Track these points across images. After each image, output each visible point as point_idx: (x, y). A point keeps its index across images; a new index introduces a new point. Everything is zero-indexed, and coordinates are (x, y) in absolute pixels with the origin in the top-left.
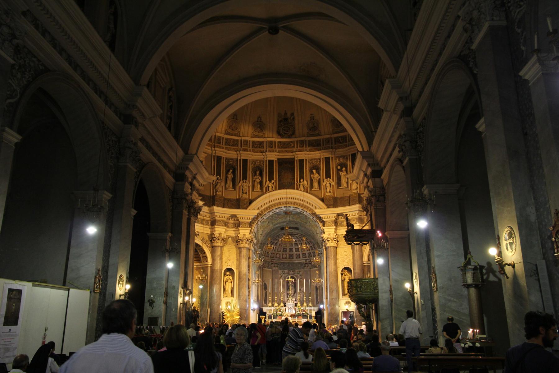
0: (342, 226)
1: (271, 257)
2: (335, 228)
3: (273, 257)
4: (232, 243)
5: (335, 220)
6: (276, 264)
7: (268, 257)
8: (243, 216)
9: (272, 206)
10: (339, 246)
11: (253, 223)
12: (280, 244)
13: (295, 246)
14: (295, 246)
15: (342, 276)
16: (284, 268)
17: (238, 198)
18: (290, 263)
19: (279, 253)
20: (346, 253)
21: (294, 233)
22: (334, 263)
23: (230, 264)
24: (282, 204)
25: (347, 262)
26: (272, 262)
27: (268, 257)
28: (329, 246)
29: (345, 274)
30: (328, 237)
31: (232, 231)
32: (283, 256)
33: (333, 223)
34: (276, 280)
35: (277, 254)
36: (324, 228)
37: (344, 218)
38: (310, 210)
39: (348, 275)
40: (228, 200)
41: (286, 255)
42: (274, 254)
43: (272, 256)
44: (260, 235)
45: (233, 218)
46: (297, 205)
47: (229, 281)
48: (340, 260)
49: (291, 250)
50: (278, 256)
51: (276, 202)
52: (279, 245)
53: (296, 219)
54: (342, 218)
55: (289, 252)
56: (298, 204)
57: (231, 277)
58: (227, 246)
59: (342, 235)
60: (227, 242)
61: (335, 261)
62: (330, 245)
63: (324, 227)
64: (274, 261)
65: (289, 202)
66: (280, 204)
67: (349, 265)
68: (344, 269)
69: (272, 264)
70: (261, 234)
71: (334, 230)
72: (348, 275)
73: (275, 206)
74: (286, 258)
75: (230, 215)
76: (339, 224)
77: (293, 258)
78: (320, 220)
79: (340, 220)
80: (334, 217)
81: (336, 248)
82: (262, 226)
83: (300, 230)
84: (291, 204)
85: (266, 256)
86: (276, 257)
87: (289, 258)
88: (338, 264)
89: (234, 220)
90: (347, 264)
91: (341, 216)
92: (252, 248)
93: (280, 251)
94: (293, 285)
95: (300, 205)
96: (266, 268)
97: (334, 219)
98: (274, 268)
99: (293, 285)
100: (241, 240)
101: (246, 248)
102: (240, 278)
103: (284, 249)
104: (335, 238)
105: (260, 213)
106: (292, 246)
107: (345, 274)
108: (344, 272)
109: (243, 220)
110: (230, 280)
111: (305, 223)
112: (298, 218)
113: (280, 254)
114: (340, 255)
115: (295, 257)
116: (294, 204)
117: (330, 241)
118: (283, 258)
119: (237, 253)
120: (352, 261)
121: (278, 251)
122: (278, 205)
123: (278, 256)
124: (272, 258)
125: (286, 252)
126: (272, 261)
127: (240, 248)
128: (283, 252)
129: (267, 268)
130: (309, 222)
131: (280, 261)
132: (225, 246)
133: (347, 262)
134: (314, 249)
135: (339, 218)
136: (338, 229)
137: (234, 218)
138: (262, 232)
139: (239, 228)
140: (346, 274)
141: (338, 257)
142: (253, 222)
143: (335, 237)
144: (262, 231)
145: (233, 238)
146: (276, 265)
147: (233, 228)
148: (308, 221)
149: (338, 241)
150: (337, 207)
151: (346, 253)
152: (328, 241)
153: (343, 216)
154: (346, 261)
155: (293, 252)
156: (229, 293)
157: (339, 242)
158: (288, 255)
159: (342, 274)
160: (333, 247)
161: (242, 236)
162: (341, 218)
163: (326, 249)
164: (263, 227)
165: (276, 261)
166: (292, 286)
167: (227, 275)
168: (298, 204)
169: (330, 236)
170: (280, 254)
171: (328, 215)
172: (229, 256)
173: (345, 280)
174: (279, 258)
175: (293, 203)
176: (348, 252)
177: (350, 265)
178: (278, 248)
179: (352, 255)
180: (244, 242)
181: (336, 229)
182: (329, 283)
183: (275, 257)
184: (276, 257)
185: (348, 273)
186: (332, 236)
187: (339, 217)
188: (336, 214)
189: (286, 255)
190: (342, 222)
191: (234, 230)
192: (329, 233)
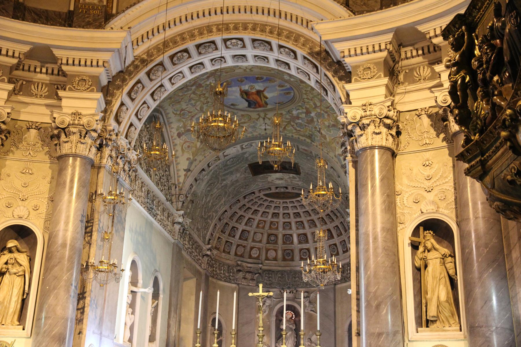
0: (414, 82)
1: (236, 254)
2: (387, 86)
3: (242, 256)
4: (39, 145)
5: (386, 61)
6: (250, 272)
7: (229, 253)
8: (77, 55)
9: (185, 36)
10: (402, 146)
11: (119, 88)
12: (258, 224)
13: (297, 228)
14: (297, 228)
15: (413, 255)
16: (270, 284)
17: (72, 8)
18: (285, 271)
19: (258, 245)
20: (428, 172)
21: (290, 190)
22: (384, 202)
23: (21, 214)
24: (214, 29)
25: (433, 202)
26: (239, 268)
27: (229, 253)
28: (364, 145)
29: (425, 247)
30: (363, 114)
31: (44, 108)
32: (268, 255)
33: (379, 71)
34: (218, 293)
35: (252, 248)
36: (348, 87)
37: (420, 52)
38: (303, 45)
39: (436, 249)
40: (37, 15)
41: (276, 251)
42: (244, 247)
43: (239, 253)
44: (182, 173)
45: (47, 65)
46: (263, 31)
47: (14, 270)
48: (406, 196)
49: (288, 239)
50: (255, 253)
51: (197, 23)
52: (258, 227)
53: (285, 128)
54: (414, 53)
55: (284, 243)
56: (268, 28)
57: (23, 259)
58: (18, 154)
59: (414, 112)
60: (20, 141)
61: (388, 196)
62: (370, 143)
63: (350, 82)
64: (244, 264)
65: (239, 23)
66: (210, 31)
67: (440, 210)
68: (421, 229)
69: (239, 271)
70: (186, 168)
71: (383, 91)
72: (436, 249)
73: (192, 36)
74: (275, 259)
75: (26, 49)
76: (401, 77)
77: (292, 260)
78: (335, 73)
79: (405, 62)
80: (383, 47)
81: (394, 155)
82: (188, 144)
83: (302, 174)
84: (245, 28)
85: (222, 249)
86: (250, 257)
87: (284, 259)
88: (398, 211)
89: (52, 74)
90: (431, 208)
91: (411, 48)
92: (107, 162)
93: (260, 242)
94: (291, 326)
95: (271, 32)
96: (221, 280)
97: (385, 54)
98: (244, 282)
99: (291, 326)
100: (64, 129)
101: (81, 157)
102: (48, 257)
103: (269, 235)
104: (387, 117)
105: (145, 57)
106: (291, 228)
107: (425, 247)
108: (421, 239)
109: (76, 69)
110: (18, 267)
111: (308, 140)
112: (289, 123)
113: (259, 249)
114: (405, 181)
115: (297, 257)
116: (254, 29)
117: (371, 129)
118: (267, 259)
119: (52, 178)
120: (451, 198)
121: (254, 241)
122: (201, 34)
123: (255, 253)
124: (238, 258)
125: (276, 243)
126: (238, 265)
127: (62, 158)
128: (268, 243)
129: (225, 281)
130: (319, 132)
131: (260, 265)
132: (11, 154)
133: (433, 202)
134: (343, 232)
135: (403, 56)
136: (399, 91)
137: (50, 66)
138: (191, 164)
139: (61, 93)
140: (429, 245)
141: (398, 187)
142: (118, 82)
143: (385, 112)
144: (188, 159)
145: (46, 129)
146: (249, 276)
147: (47, 97)
148: (316, 128)
149: (399, 133)
150: (395, 4)
151: (428, 172)
152: (363, 128)
153: (416, 46)
154: (431, 196)
155: (292, 243)
156: (11, 310)
157: (401, 137)
158: (280, 253)
159: (415, 247)
160: (381, 147)
161: (68, 120)
162: (409, 55)
163: (355, 164)
164: (189, 147)
165: (249, 265)
166: (291, 329)
167: (10, 251)
168: (268, 28)
169: (368, 113)
170: (259, 249)
171: (364, 42)
172: (25, 186)
173: (426, 266)
174: (258, 258)
175: (250, 26)
176: (436, 166)
177: (446, 212)
178: (255, 233)
179: (452, 175)
180: (74, 138)
181: (391, 93)
182: (366, 273)
183: (246, 255)
184: (250, 257)
185: (439, 242)
186: (376, 111)
187: (403, 50)
188: (389, 37)
189: (276, 251)
190: (412, 70)
191: (47, 106)
192: (364, 102)
